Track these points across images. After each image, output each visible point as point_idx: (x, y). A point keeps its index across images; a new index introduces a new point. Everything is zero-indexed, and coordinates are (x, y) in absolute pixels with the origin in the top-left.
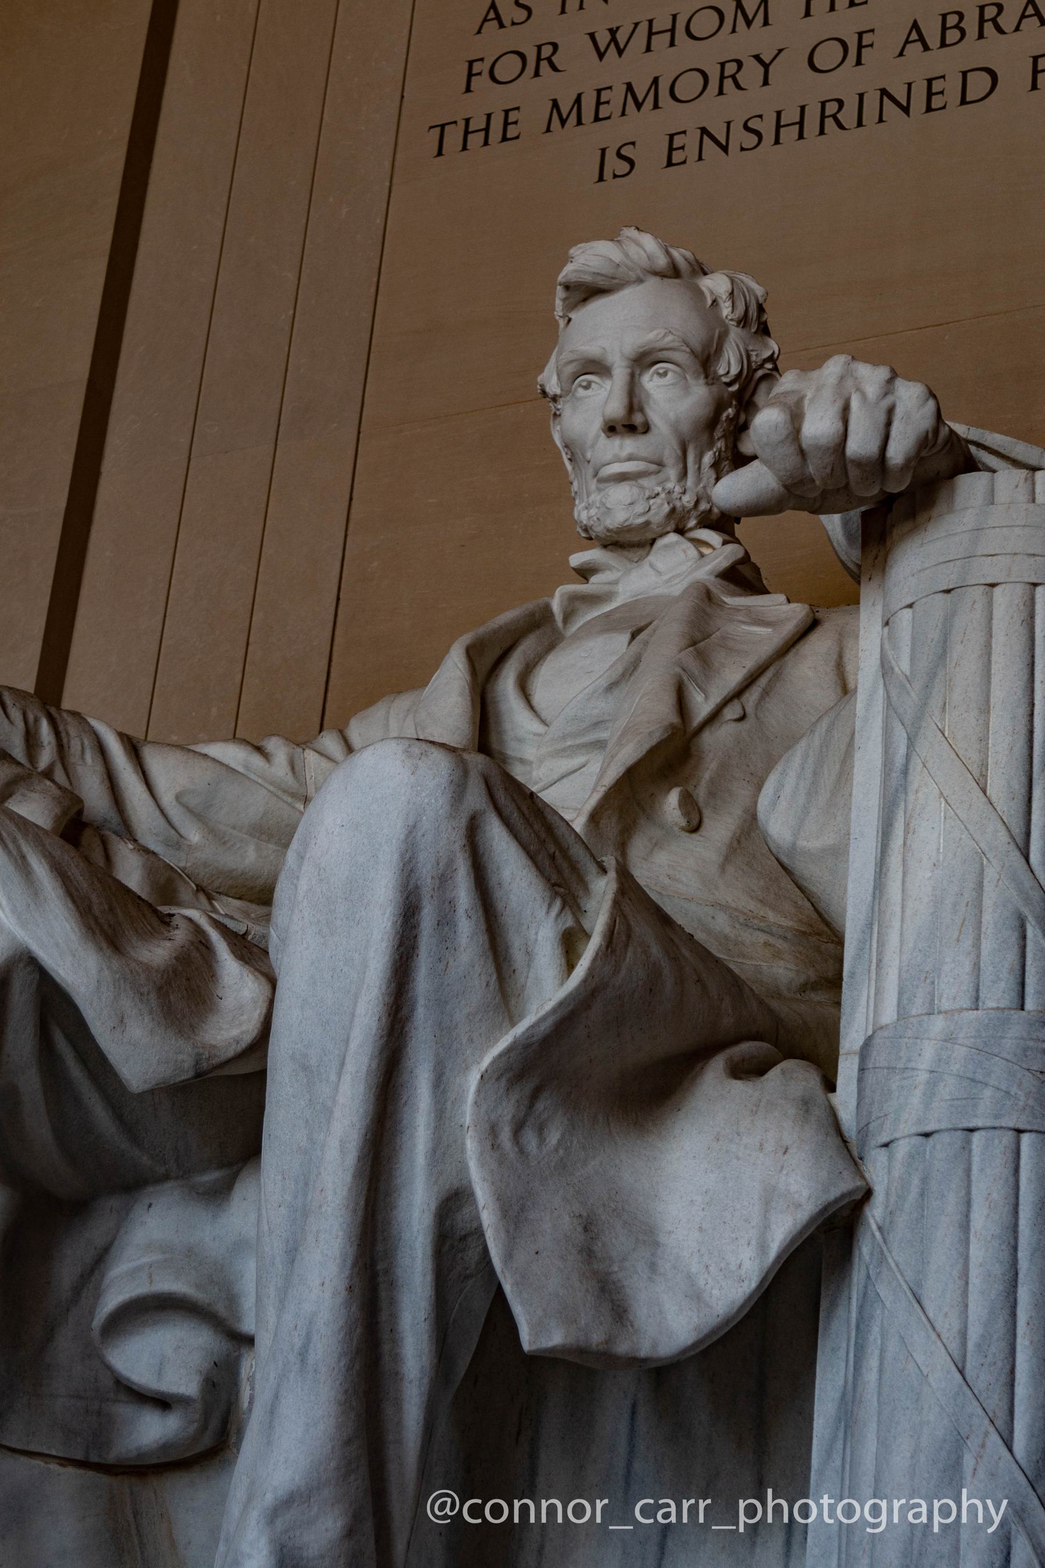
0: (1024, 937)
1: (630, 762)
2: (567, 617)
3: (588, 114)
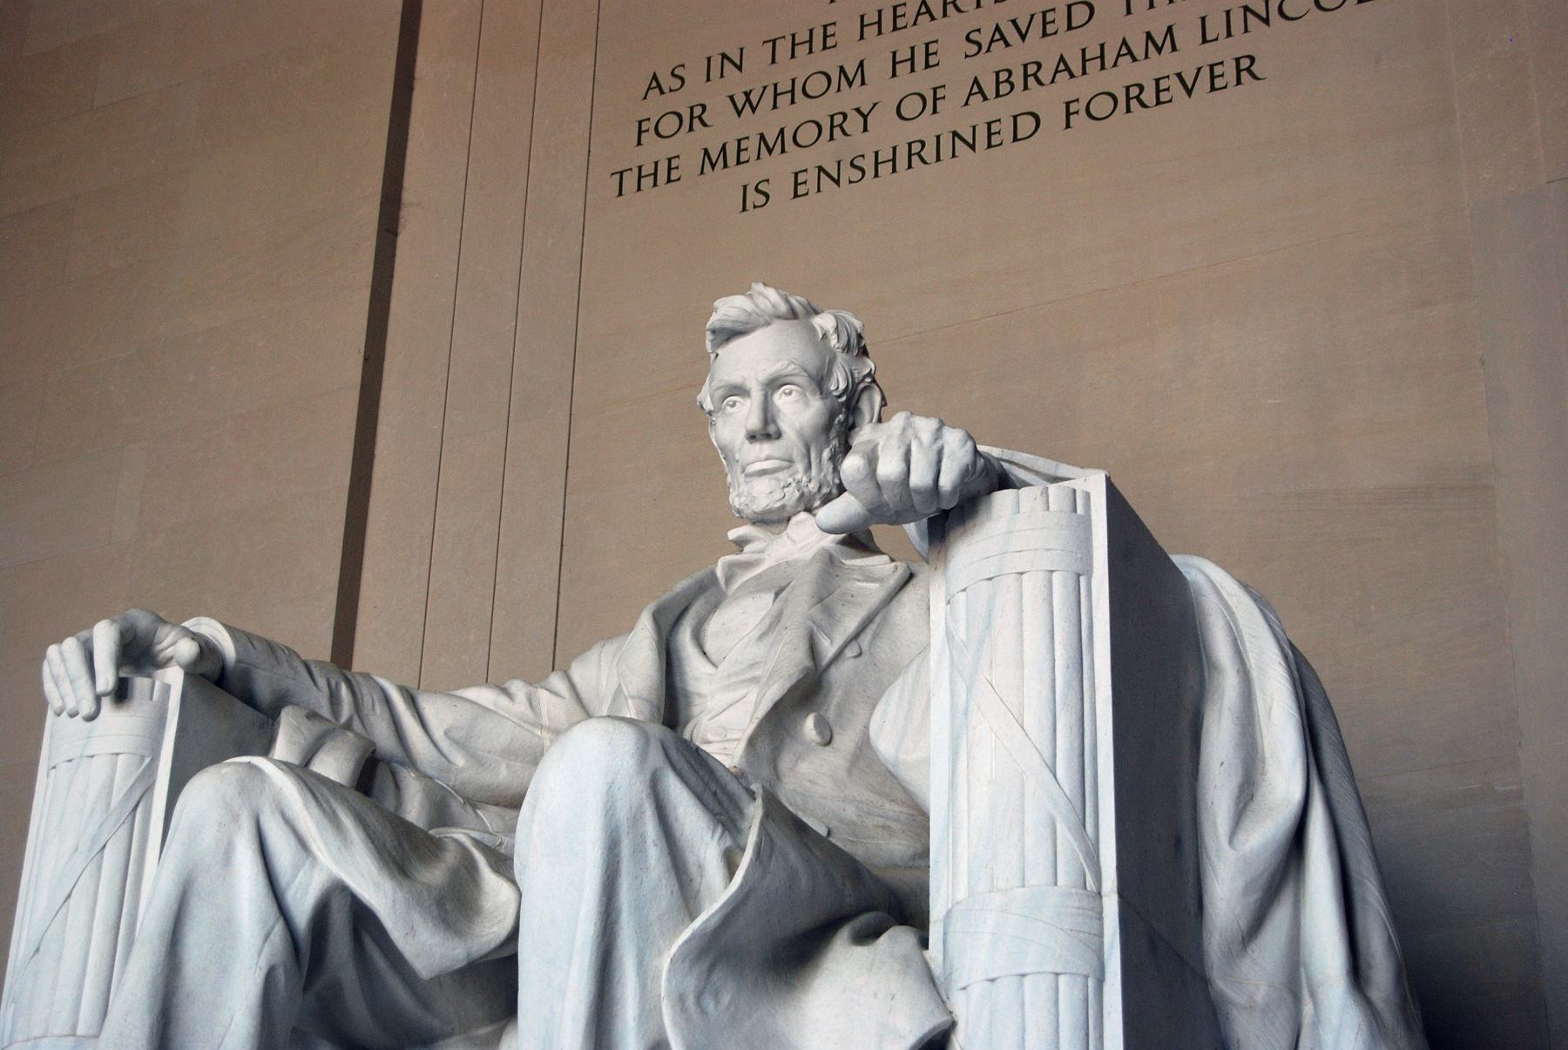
0: (1055, 832)
1: (777, 698)
2: (728, 580)
3: (732, 159)
